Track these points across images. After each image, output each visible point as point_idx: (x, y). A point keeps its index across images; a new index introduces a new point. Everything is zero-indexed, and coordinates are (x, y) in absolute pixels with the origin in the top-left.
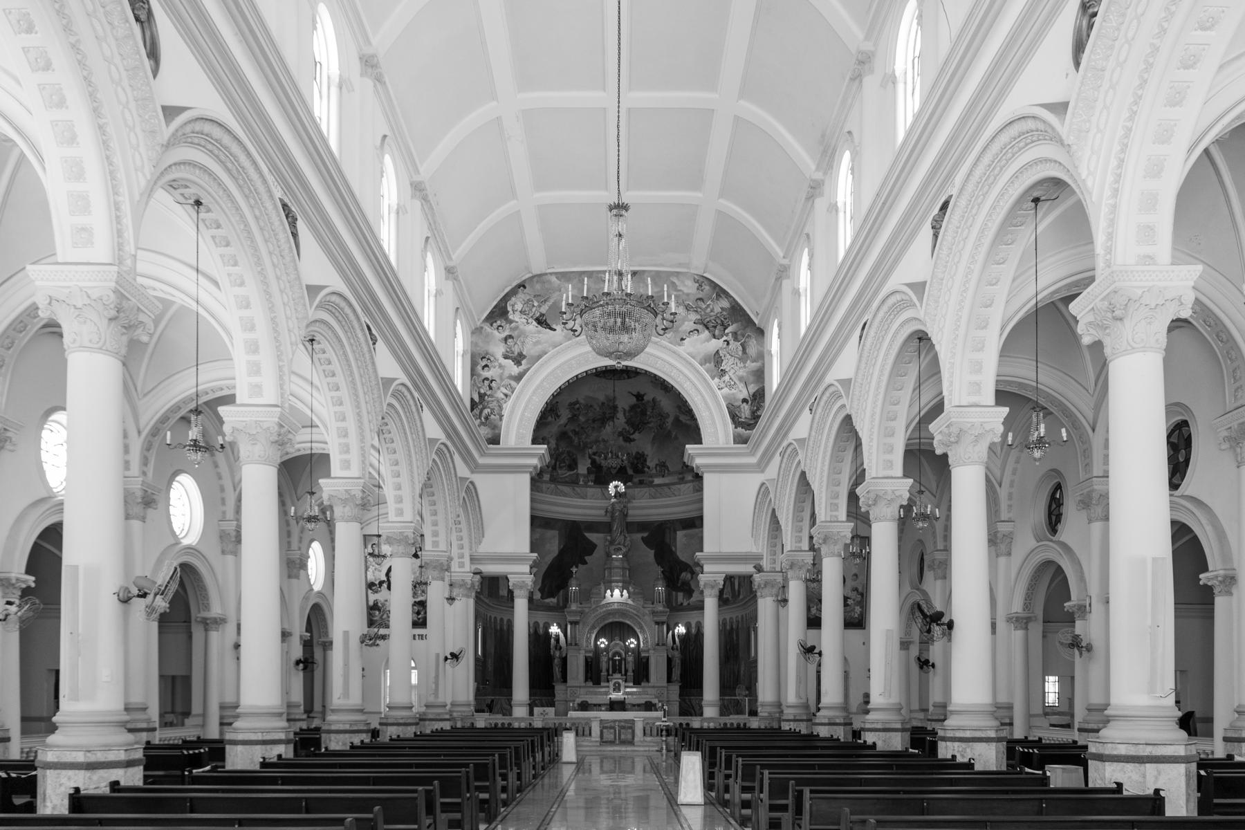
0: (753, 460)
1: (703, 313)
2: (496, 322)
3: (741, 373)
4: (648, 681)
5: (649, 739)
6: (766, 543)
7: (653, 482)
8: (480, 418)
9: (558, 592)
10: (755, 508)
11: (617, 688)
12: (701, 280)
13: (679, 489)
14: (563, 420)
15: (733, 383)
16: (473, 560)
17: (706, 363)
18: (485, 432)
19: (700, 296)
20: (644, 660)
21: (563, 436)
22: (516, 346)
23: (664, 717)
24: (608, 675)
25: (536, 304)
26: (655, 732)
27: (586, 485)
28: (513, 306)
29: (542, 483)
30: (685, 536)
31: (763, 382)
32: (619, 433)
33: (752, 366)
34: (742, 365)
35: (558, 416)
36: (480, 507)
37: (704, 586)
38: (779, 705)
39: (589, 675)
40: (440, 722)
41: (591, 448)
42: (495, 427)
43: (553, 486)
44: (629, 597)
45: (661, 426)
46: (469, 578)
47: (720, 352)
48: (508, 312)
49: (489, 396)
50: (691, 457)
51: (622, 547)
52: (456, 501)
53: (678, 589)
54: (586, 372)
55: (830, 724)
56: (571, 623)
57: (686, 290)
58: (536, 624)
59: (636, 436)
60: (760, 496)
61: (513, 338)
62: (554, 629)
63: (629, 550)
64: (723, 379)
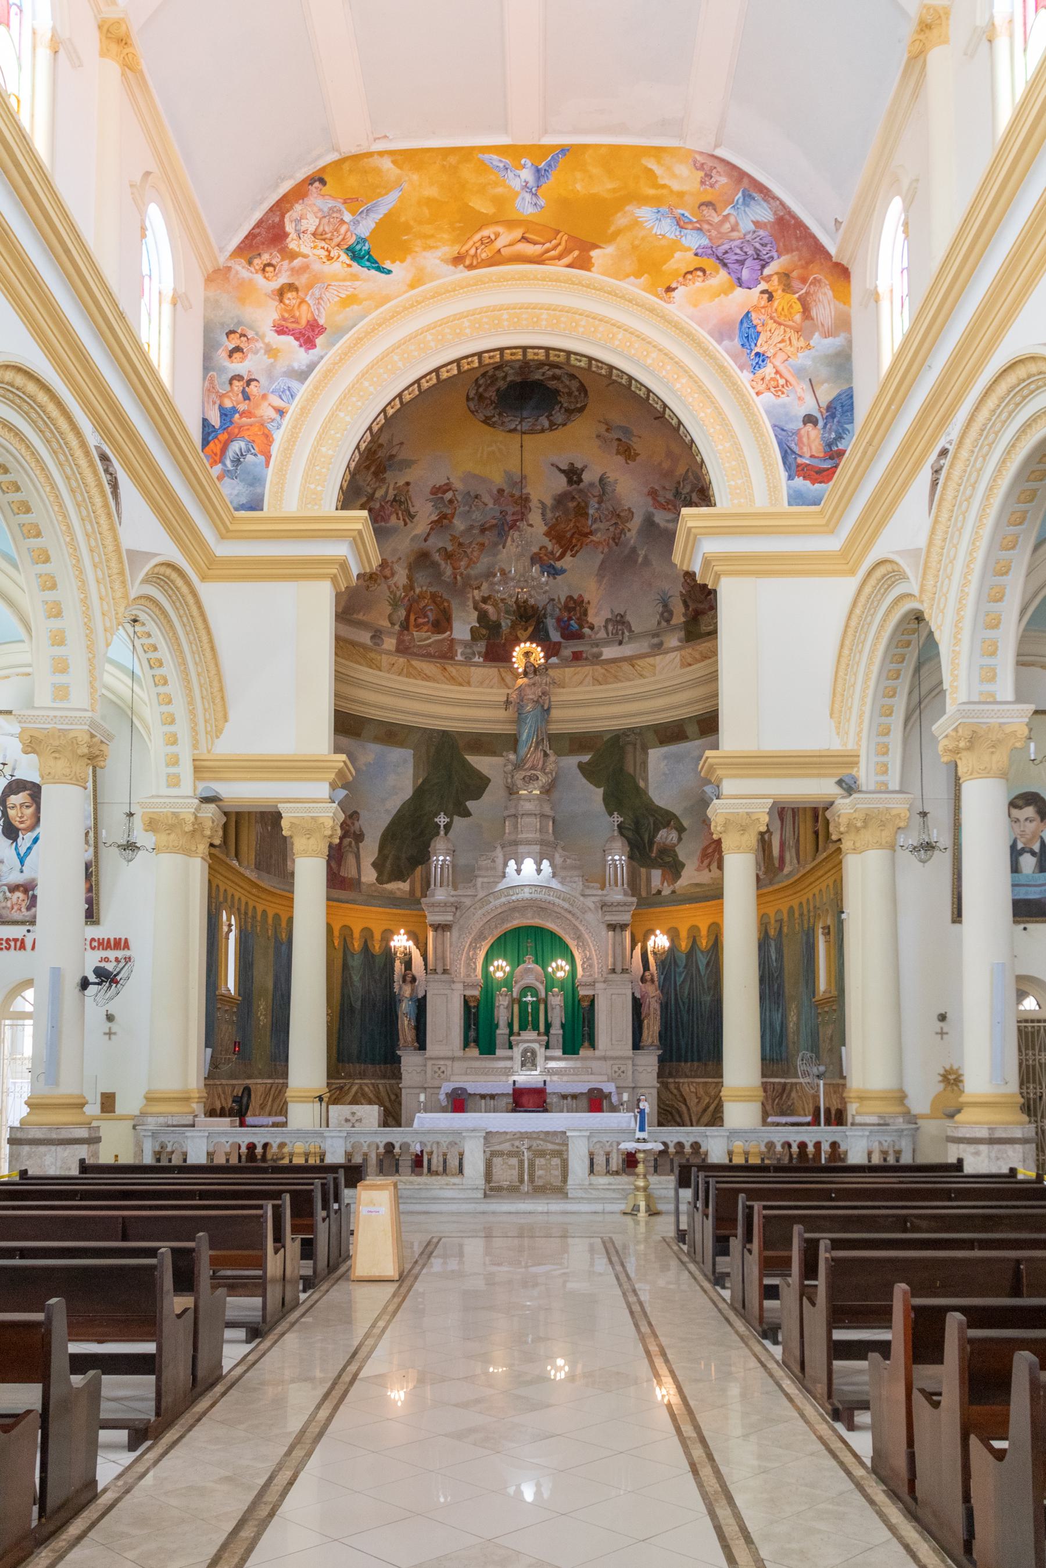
0: (833, 544)
1: (714, 233)
2: (259, 255)
3: (803, 359)
4: (593, 1046)
5: (603, 1181)
6: (866, 725)
7: (601, 654)
8: (221, 460)
9: (413, 869)
10: (842, 646)
11: (529, 1060)
12: (710, 163)
13: (654, 666)
14: (421, 526)
15: (782, 382)
16: (200, 769)
17: (722, 340)
18: (231, 490)
19: (707, 198)
20: (586, 1004)
21: (422, 560)
22: (304, 307)
23: (642, 1129)
24: (511, 1033)
25: (347, 217)
26: (616, 1163)
27: (468, 661)
28: (298, 221)
29: (380, 653)
30: (665, 757)
31: (850, 379)
32: (535, 554)
33: (823, 344)
34: (802, 343)
35: (412, 517)
36: (213, 648)
37: (725, 825)
38: (900, 1097)
39: (472, 1034)
40: (60, 1148)
41: (478, 588)
42: (256, 481)
43: (402, 661)
44: (554, 875)
45: (616, 540)
46: (188, 808)
47: (754, 315)
48: (286, 235)
49: (242, 414)
50: (693, 539)
51: (538, 773)
52: (117, 585)
53: (652, 864)
54: (458, 361)
55: (992, 1141)
56: (438, 928)
57: (676, 186)
58: (367, 932)
59: (567, 562)
60: (857, 611)
61: (297, 290)
62: (401, 942)
63: (554, 780)
64: (760, 372)
